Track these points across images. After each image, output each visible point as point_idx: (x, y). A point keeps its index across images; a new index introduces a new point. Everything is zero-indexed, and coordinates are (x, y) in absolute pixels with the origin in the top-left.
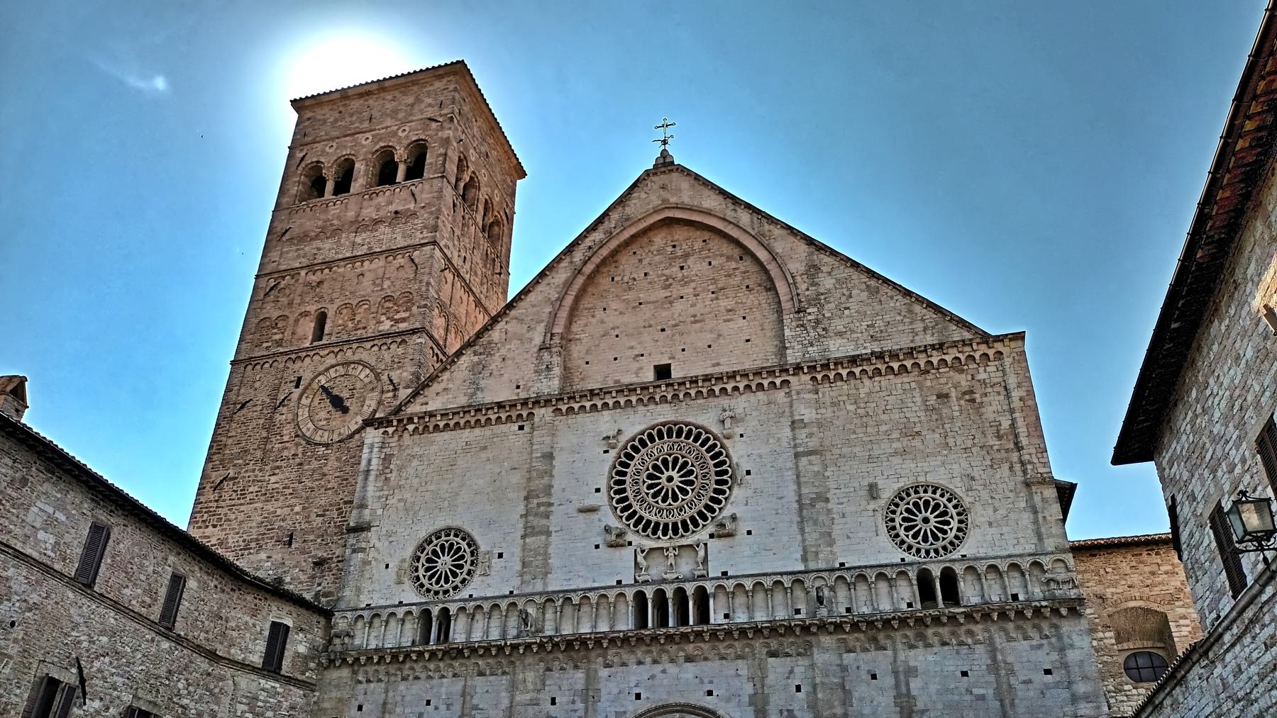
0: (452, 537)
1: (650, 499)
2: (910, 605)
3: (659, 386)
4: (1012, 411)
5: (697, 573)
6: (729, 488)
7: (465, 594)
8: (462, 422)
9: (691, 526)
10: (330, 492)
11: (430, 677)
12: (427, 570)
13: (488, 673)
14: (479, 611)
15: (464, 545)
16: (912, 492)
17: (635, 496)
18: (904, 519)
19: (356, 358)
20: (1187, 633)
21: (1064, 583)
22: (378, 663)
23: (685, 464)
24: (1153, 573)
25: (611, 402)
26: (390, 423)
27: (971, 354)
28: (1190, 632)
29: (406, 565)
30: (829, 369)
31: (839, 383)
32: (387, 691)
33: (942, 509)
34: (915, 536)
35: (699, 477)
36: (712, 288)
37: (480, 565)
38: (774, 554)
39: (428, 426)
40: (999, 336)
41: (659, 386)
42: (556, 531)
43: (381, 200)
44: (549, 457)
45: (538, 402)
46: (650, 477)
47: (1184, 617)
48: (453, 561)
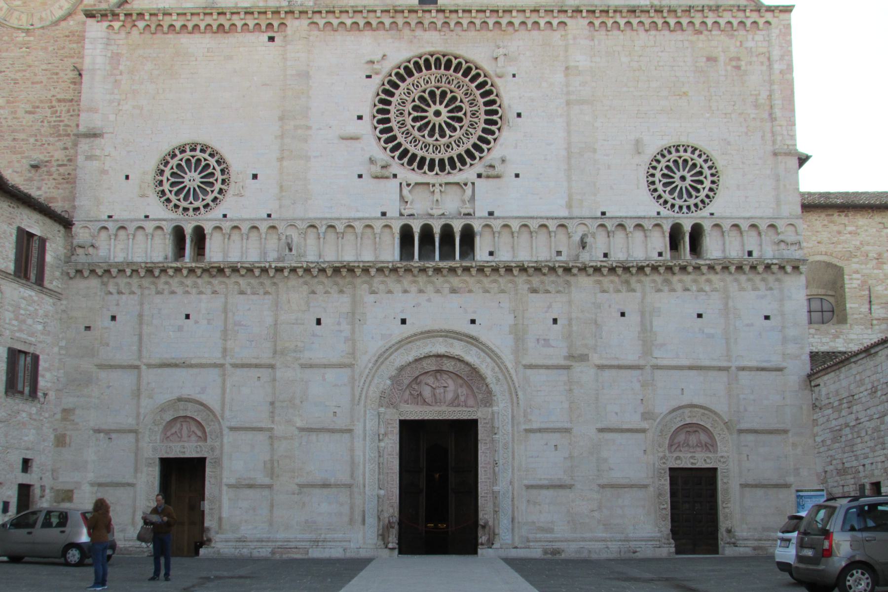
0: (198, 153)
1: (416, 133)
2: (660, 254)
3: (430, 11)
4: (771, 83)
5: (464, 211)
6: (499, 129)
7: (217, 212)
8: (202, 26)
9: (458, 164)
10: (38, 86)
11: (187, 292)
12: (173, 184)
13: (249, 291)
14: (236, 231)
15: (212, 161)
16: (673, 150)
17: (399, 128)
18: (664, 175)
20: (856, 286)
21: (792, 244)
22: (130, 276)
23: (454, 99)
24: (839, 233)
25: (374, 23)
26: (115, 15)
27: (744, 20)
28: (859, 285)
29: (150, 177)
30: (609, 17)
31: (616, 32)
32: (142, 304)
33: (698, 169)
34: (672, 192)
35: (469, 114)
37: (232, 185)
38: (541, 198)
39: (161, 26)
40: (770, 7)
41: (430, 11)
42: (315, 157)
44: (305, 75)
45: (292, 12)
46: (416, 108)
47: (857, 272)
48: (202, 178)
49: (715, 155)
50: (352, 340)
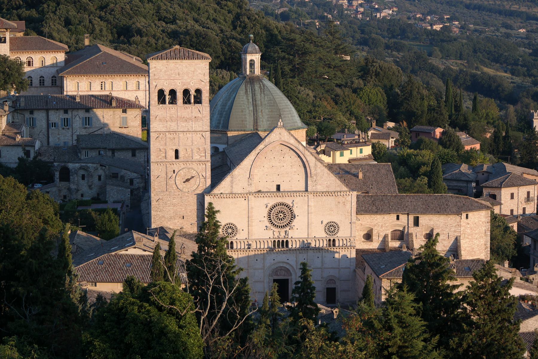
1: (276, 220)
7: (235, 238)
15: (234, 227)
19: (190, 166)
23: (284, 212)
36: (291, 165)
43: (189, 110)
49: (338, 223)
50: (264, 264)
